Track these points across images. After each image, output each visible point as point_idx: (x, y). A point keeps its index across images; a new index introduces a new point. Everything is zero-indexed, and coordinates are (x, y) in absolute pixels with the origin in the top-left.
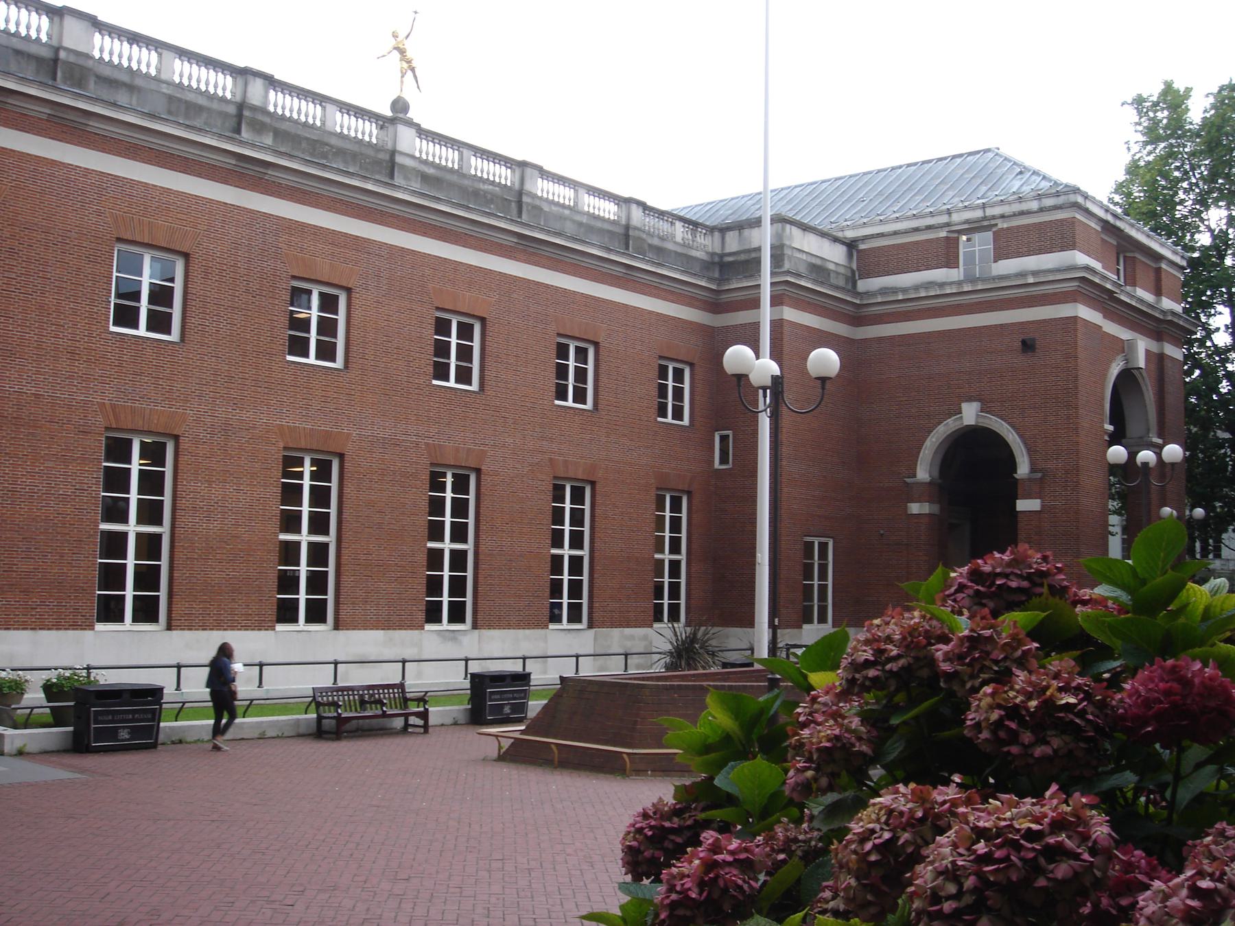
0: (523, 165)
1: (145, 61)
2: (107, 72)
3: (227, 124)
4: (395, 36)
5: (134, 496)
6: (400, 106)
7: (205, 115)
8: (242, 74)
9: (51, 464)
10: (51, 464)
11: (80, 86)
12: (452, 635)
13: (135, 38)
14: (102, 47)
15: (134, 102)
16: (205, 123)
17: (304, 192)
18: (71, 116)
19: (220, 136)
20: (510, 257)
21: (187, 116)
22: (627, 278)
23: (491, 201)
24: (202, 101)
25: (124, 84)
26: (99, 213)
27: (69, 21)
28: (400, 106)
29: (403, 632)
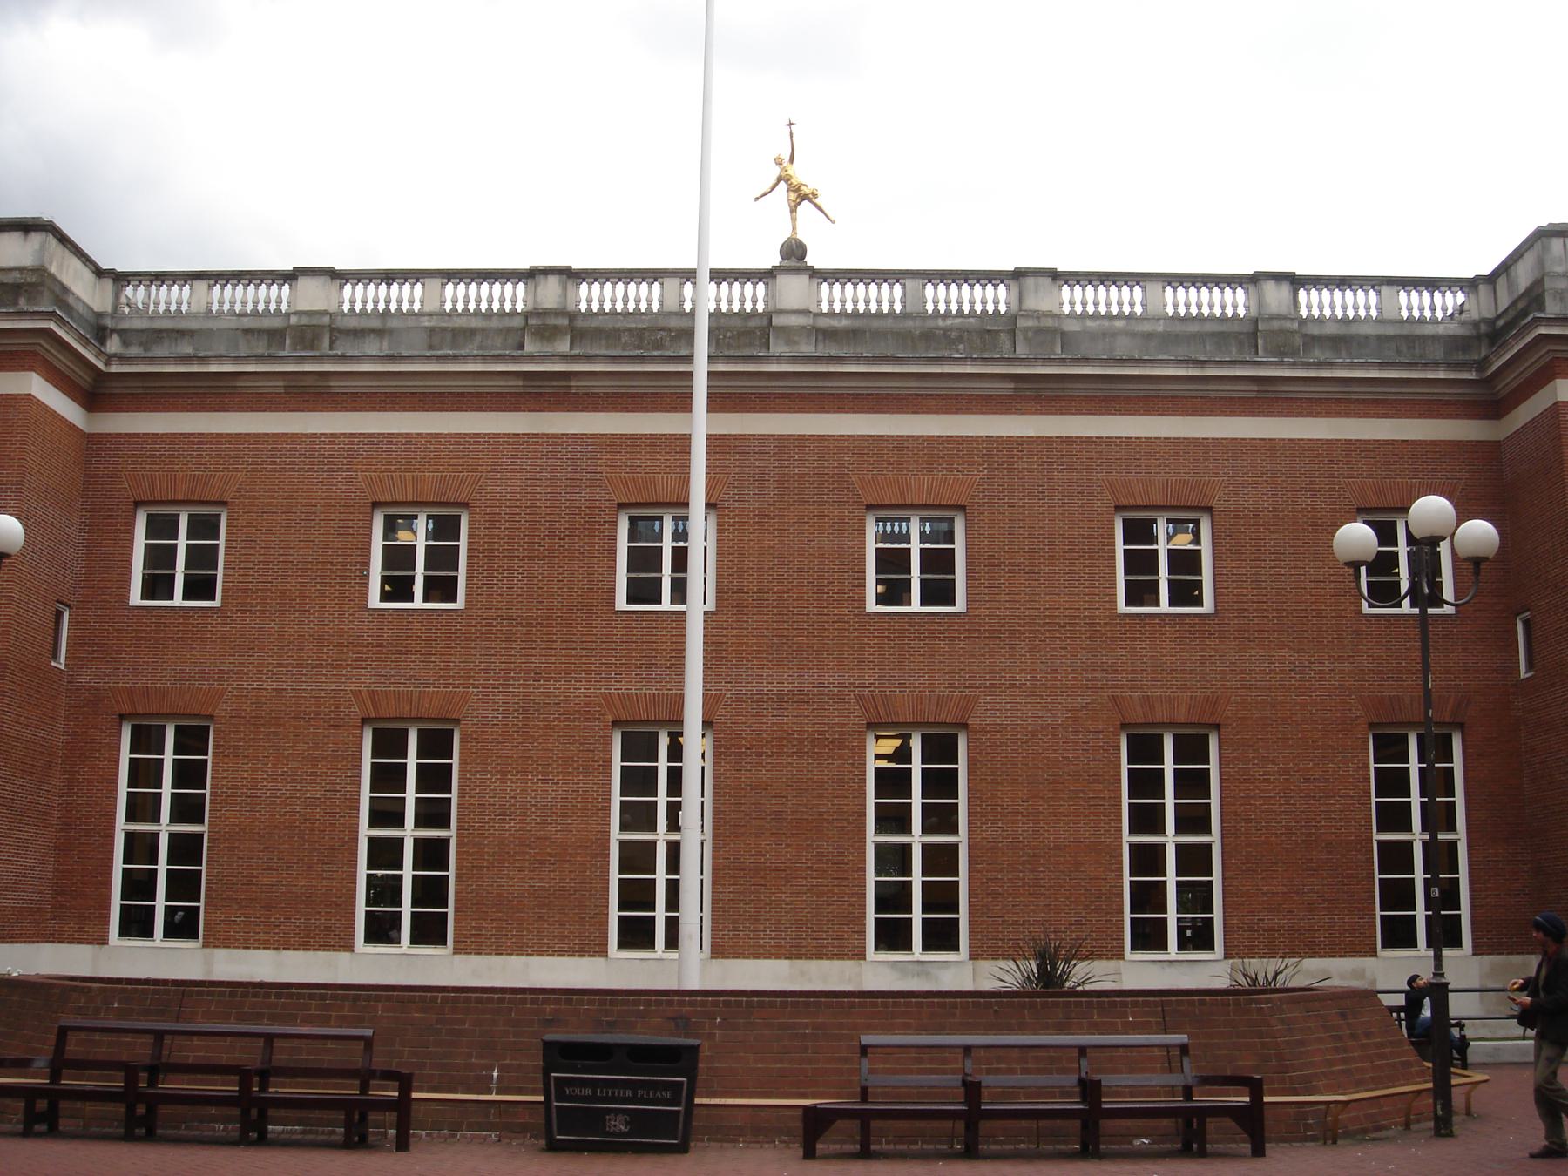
0: (1018, 275)
1: (410, 297)
2: (353, 323)
3: (510, 341)
4: (779, 161)
5: (411, 795)
6: (794, 252)
7: (478, 338)
8: (531, 275)
9: (295, 765)
10: (295, 765)
11: (312, 349)
12: (916, 967)
13: (389, 277)
14: (355, 297)
15: (385, 344)
16: (480, 348)
17: (633, 396)
18: (309, 382)
19: (484, 357)
20: (1008, 411)
21: (454, 346)
22: (1266, 398)
23: (960, 339)
24: (475, 323)
25: (373, 331)
26: (349, 479)
27: (303, 282)
28: (794, 252)
29: (825, 963)
